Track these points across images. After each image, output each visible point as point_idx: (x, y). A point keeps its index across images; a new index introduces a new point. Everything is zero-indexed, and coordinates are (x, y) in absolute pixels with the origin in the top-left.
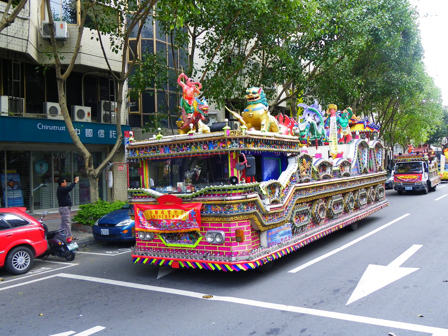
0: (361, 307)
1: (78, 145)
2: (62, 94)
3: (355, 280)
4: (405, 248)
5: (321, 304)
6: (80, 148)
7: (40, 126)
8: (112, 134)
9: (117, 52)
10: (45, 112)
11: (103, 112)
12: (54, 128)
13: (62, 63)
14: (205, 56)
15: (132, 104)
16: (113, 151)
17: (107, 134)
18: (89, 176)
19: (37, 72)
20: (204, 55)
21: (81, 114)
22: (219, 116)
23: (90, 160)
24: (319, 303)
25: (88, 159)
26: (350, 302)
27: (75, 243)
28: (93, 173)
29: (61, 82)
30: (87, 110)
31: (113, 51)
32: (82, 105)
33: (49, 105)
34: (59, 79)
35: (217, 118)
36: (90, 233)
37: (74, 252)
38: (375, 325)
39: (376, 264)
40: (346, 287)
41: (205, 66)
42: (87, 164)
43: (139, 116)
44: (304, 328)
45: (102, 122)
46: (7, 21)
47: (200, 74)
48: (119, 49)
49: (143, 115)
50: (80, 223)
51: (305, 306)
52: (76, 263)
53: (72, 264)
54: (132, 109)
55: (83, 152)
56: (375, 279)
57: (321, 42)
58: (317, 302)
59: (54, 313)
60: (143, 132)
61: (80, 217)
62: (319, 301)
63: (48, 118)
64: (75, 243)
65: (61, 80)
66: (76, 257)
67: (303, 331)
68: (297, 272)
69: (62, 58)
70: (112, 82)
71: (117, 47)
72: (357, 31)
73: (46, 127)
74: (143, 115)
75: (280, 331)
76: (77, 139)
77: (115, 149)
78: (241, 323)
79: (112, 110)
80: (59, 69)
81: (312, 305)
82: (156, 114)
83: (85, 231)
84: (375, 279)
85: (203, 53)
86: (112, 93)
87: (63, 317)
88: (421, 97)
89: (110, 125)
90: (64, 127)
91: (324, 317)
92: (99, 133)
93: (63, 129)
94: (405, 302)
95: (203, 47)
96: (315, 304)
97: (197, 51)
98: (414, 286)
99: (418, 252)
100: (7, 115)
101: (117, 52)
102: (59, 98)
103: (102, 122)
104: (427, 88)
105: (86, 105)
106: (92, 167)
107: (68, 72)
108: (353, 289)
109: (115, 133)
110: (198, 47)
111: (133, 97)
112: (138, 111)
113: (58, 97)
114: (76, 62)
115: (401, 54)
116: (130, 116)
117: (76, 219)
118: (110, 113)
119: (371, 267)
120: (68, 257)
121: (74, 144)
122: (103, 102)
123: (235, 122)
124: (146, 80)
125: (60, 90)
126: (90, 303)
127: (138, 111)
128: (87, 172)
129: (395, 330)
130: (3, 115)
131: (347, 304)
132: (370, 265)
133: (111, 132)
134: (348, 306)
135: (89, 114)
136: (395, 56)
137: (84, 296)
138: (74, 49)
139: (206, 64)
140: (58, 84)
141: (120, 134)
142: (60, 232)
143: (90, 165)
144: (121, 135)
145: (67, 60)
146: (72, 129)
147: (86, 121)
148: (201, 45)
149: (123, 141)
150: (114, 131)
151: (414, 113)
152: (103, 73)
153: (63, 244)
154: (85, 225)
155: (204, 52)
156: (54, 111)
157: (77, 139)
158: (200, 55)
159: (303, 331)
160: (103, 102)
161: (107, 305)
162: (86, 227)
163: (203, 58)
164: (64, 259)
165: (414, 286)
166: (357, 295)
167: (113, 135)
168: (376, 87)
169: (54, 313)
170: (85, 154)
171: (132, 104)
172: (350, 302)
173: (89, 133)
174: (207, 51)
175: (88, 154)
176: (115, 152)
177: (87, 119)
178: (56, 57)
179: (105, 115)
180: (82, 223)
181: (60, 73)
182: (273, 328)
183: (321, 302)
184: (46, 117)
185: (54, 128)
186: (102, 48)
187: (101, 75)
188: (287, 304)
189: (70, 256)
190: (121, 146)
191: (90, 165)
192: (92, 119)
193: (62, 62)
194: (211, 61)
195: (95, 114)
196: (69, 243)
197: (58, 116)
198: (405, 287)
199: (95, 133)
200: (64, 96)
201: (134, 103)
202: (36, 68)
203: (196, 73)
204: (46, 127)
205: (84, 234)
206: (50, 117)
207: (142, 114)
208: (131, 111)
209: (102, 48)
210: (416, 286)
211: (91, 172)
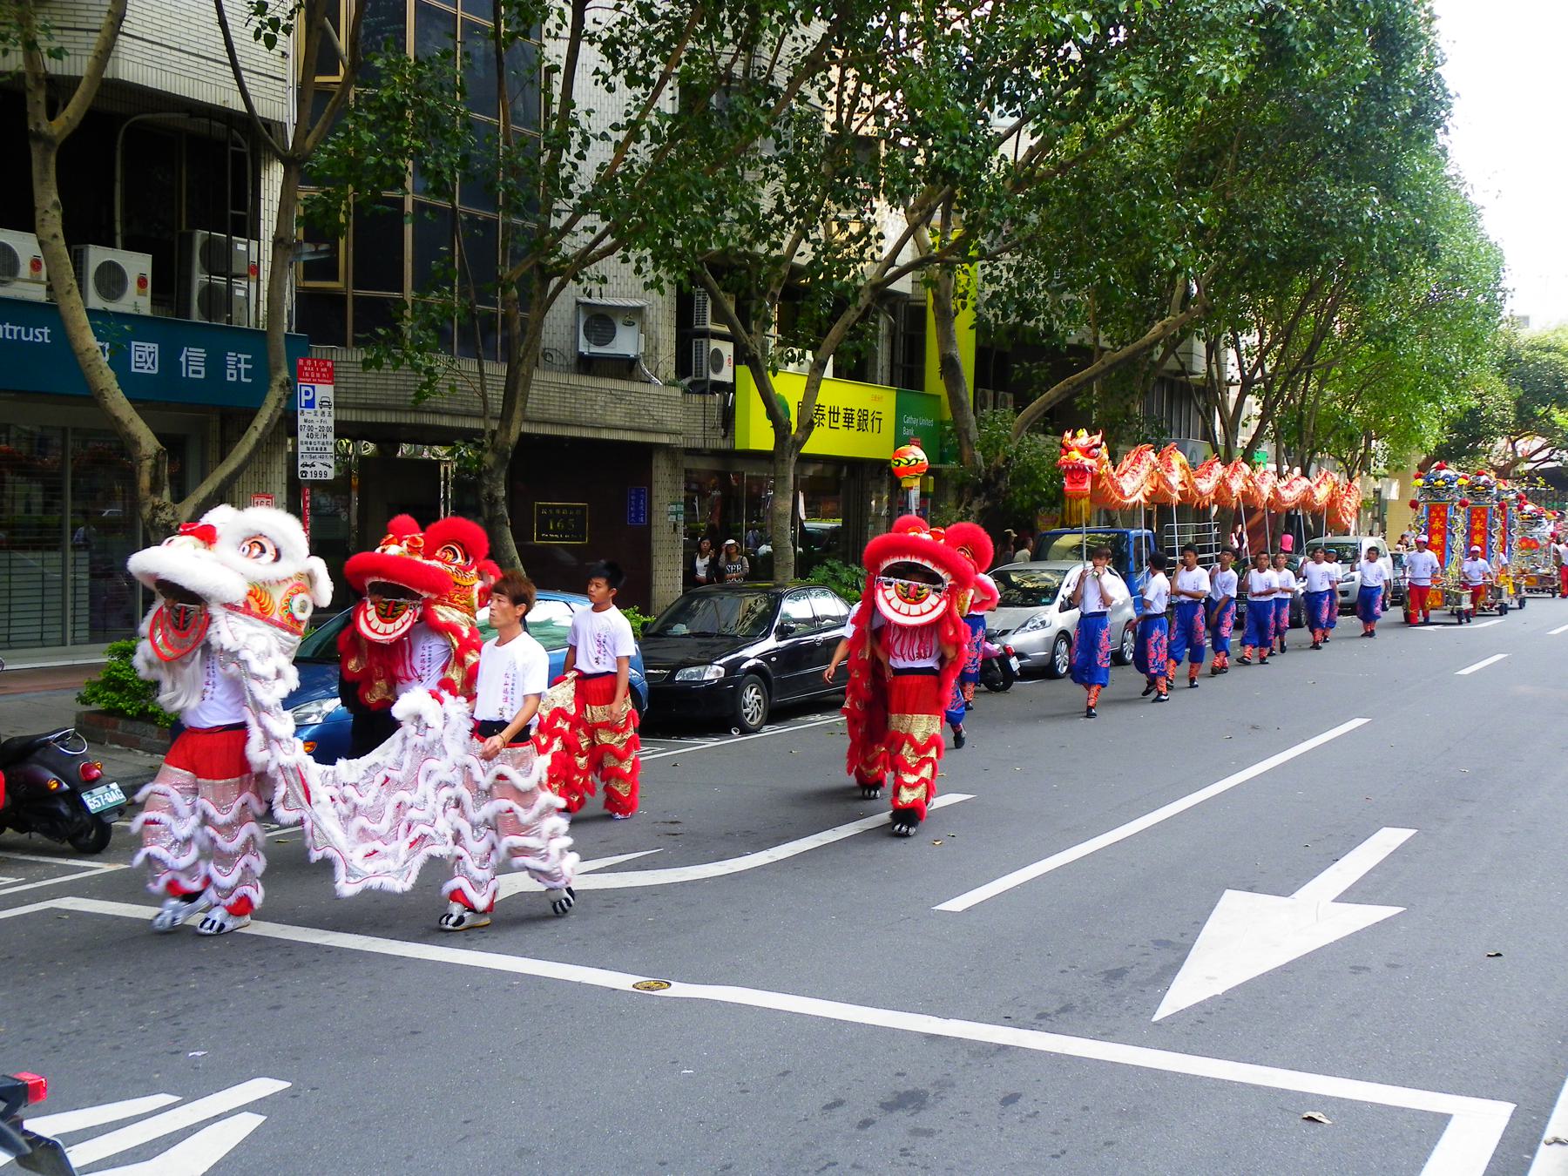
0: (1208, 1027)
1: (111, 404)
2: (48, 198)
3: (1175, 938)
4: (1353, 839)
5: (1063, 1016)
6: (117, 419)
8: (237, 366)
9: (271, 42)
11: (200, 278)
13: (53, 72)
14: (619, 80)
15: (317, 252)
16: (253, 436)
17: (216, 365)
18: (153, 528)
20: (616, 72)
21: (112, 280)
22: (651, 315)
23: (156, 467)
24: (1058, 1012)
25: (149, 463)
26: (1164, 1011)
27: (114, 786)
28: (169, 518)
29: (47, 150)
30: (138, 265)
31: (257, 35)
32: (112, 245)
34: (39, 137)
35: (643, 323)
36: (152, 752)
37: (107, 819)
38: (1257, 1088)
39: (1251, 890)
40: (1147, 964)
41: (623, 121)
42: (145, 481)
43: (338, 300)
44: (1011, 1090)
45: (196, 316)
47: (601, 153)
48: (281, 36)
49: (355, 298)
50: (114, 713)
51: (1008, 1021)
52: (115, 861)
53: (101, 867)
54: (311, 271)
55: (129, 434)
56: (1245, 939)
57: (1068, 51)
58: (1051, 1010)
59: (78, 1032)
60: (366, 364)
61: (113, 689)
62: (1057, 1006)
64: (114, 786)
65: (48, 141)
66: (114, 838)
67: (1010, 1099)
68: (969, 910)
69: (58, 54)
70: (239, 159)
71: (275, 23)
72: (1208, 17)
74: (355, 298)
75: (931, 1100)
76: (107, 380)
77: (260, 428)
78: (786, 1073)
79: (235, 270)
80: (41, 96)
81: (1031, 1018)
82: (409, 294)
83: (131, 743)
84: (1245, 939)
85: (607, 67)
86: (240, 203)
87: (117, 1048)
88: (1426, 281)
89: (223, 334)
90: (46, 331)
91: (1080, 1059)
92: (183, 359)
93: (42, 335)
94: (1357, 1015)
96: (1042, 1016)
97: (590, 56)
98: (1389, 966)
99: (1400, 853)
101: (271, 42)
102: (39, 215)
103: (196, 316)
104: (1452, 247)
105: (130, 246)
106: (166, 493)
107: (73, 112)
108: (1173, 969)
109: (247, 361)
110: (591, 42)
112: (336, 279)
113: (31, 209)
114: (108, 74)
115: (1361, 113)
116: (303, 298)
117: (95, 694)
118: (229, 283)
119: (1232, 900)
120: (82, 840)
121: (94, 398)
122: (200, 235)
123: (715, 344)
124: (388, 163)
125: (43, 181)
126: (212, 1003)
127: (336, 279)
128: (146, 512)
129: (1325, 1101)
131: (1155, 1018)
132: (1229, 894)
133: (231, 357)
134: (1158, 1024)
135: (142, 282)
136: (1341, 119)
137: (179, 976)
138: (100, 20)
139: (628, 114)
141: (279, 368)
142: (56, 740)
143: (156, 488)
144: (284, 374)
145: (77, 64)
146: (88, 340)
147: (129, 310)
148: (605, 36)
149: (292, 397)
150: (242, 357)
151: (1394, 340)
152: (206, 121)
153: (65, 786)
154: (131, 718)
155: (615, 64)
157: (107, 380)
158: (597, 72)
159: (1010, 1099)
160: (200, 235)
161: (277, 1008)
162: (139, 727)
163: (611, 89)
164: (67, 845)
165: (1389, 966)
166: (1187, 990)
167: (238, 370)
168: (1261, 235)
169: (78, 1032)
170: (137, 443)
171: (317, 252)
172: (1164, 1011)
173: (145, 356)
174: (627, 59)
175: (148, 443)
176: (258, 441)
177: (136, 301)
178: (30, 46)
179: (209, 289)
180: (121, 713)
181: (42, 111)
182: (902, 1090)
183: (1064, 1010)
186: (223, 23)
187: (200, 125)
188: (946, 1014)
189: (93, 836)
190: (281, 418)
191: (156, 488)
192: (154, 302)
193: (54, 67)
194: (649, 105)
195: (168, 283)
196: (92, 783)
197: (18, 284)
198: (1356, 970)
199: (169, 359)
200: (55, 205)
201: (323, 247)
203: (586, 143)
205: (128, 757)
207: (351, 293)
208: (307, 277)
209: (223, 23)
210: (1395, 966)
211: (162, 515)
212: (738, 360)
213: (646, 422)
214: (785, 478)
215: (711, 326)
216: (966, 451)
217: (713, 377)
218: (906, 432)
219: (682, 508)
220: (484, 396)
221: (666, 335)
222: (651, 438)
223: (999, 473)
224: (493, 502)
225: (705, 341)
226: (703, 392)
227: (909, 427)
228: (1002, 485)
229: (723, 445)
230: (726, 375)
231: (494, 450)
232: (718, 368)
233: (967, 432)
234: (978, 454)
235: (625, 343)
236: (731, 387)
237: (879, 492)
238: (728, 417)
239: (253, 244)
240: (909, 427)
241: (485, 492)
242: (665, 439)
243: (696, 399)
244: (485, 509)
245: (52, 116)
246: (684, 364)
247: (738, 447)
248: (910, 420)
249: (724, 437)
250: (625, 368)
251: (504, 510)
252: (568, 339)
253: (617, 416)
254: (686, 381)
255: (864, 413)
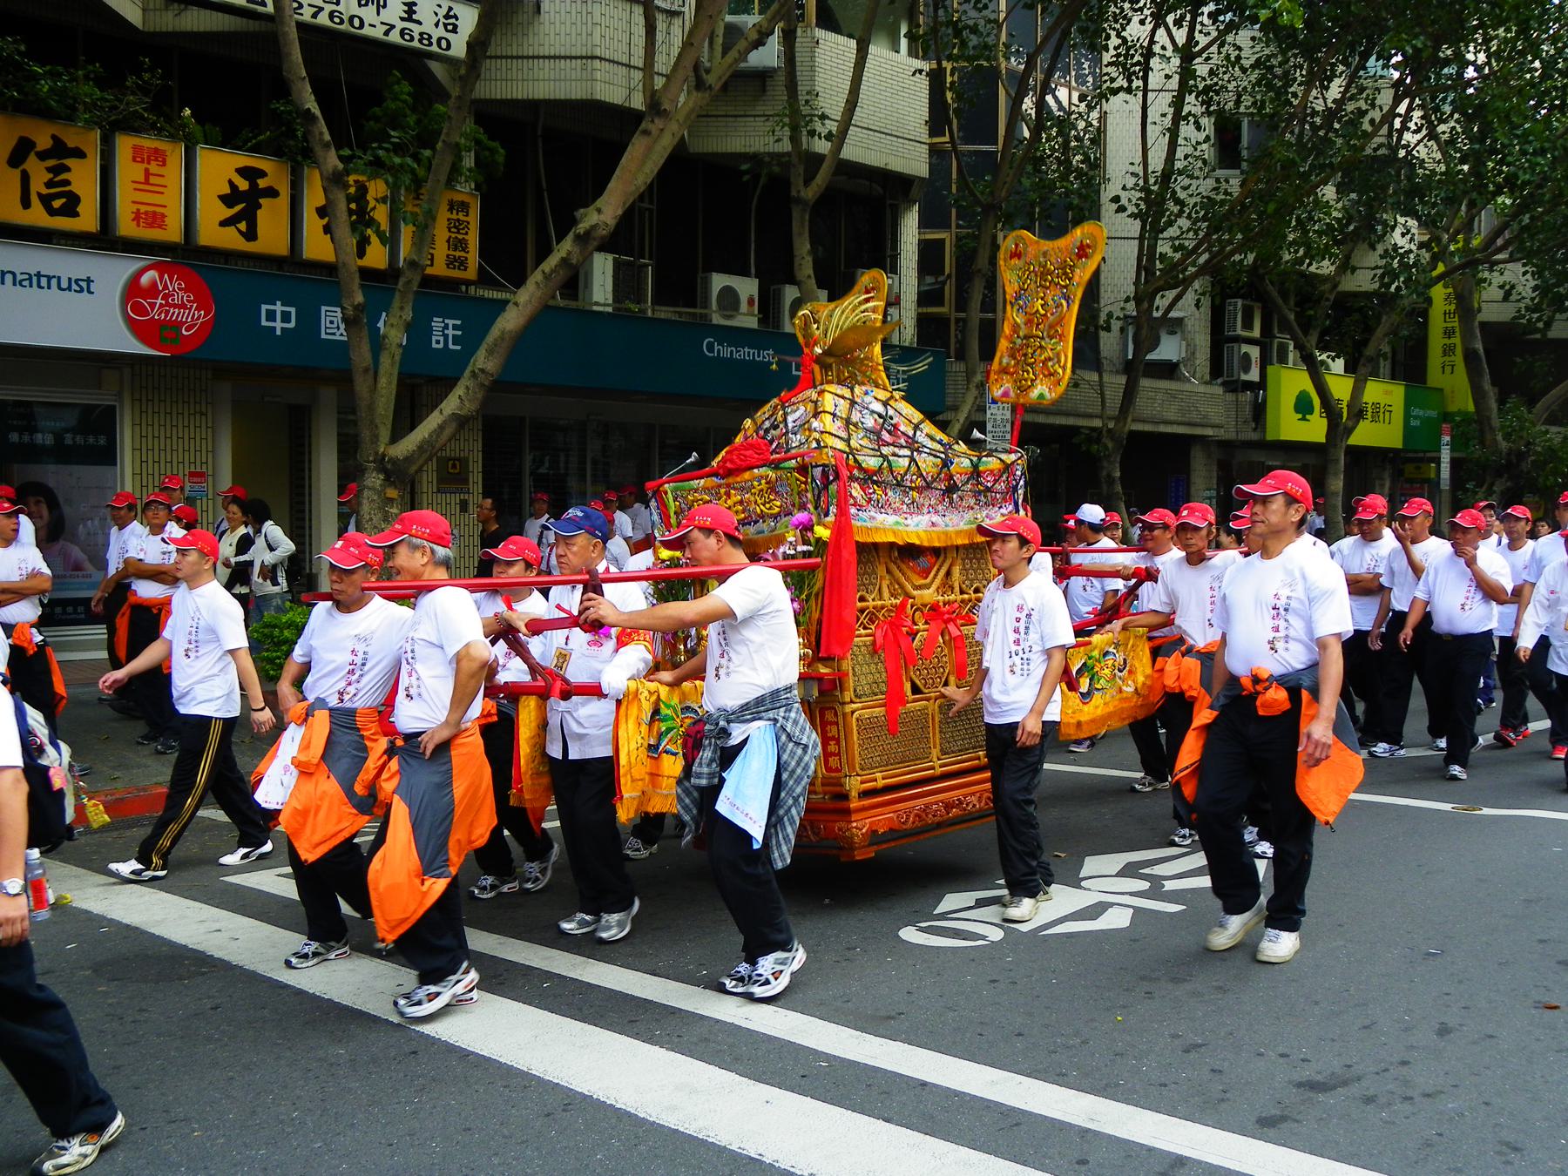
7: (710, 348)
10: (706, 303)
12: (746, 353)
19: (746, 178)
22: (1189, 323)
33: (719, 281)
34: (799, 201)
46: (759, 32)
63: (715, 322)
73: (726, 351)
80: (801, 170)
95: (1207, 89)
100: (610, 309)
111: (929, 256)
123: (1245, 348)
125: (800, 234)
130: (595, 308)
140: (796, 213)
141: (974, 373)
156: (729, 299)
181: (801, 182)
184: (705, 317)
185: (746, 353)
197: (740, 317)
202: (744, 167)
204: (726, 351)
206: (717, 319)
212: (1265, 362)
213: (1195, 417)
214: (1337, 461)
215: (1239, 331)
216: (1488, 437)
217: (1244, 377)
218: (1414, 423)
219: (1214, 493)
220: (1102, 394)
221: (1203, 340)
222: (1198, 431)
223: (1521, 456)
224: (1110, 481)
225: (1236, 346)
226: (1234, 391)
227: (1416, 417)
228: (1526, 465)
229: (1254, 436)
230: (1254, 375)
231: (1112, 439)
232: (1247, 369)
233: (1489, 419)
234: (1499, 438)
235: (1168, 349)
236: (1262, 384)
237: (1382, 479)
238: (1259, 412)
239: (896, 278)
240: (1416, 417)
241: (1104, 473)
242: (1209, 432)
243: (1230, 397)
244: (1105, 487)
245: (807, 182)
246: (1217, 368)
247: (1270, 437)
248: (1416, 412)
249: (1255, 430)
250: (1168, 370)
251: (1119, 488)
252: (1117, 348)
253: (1171, 415)
254: (1219, 381)
255: (1376, 405)
